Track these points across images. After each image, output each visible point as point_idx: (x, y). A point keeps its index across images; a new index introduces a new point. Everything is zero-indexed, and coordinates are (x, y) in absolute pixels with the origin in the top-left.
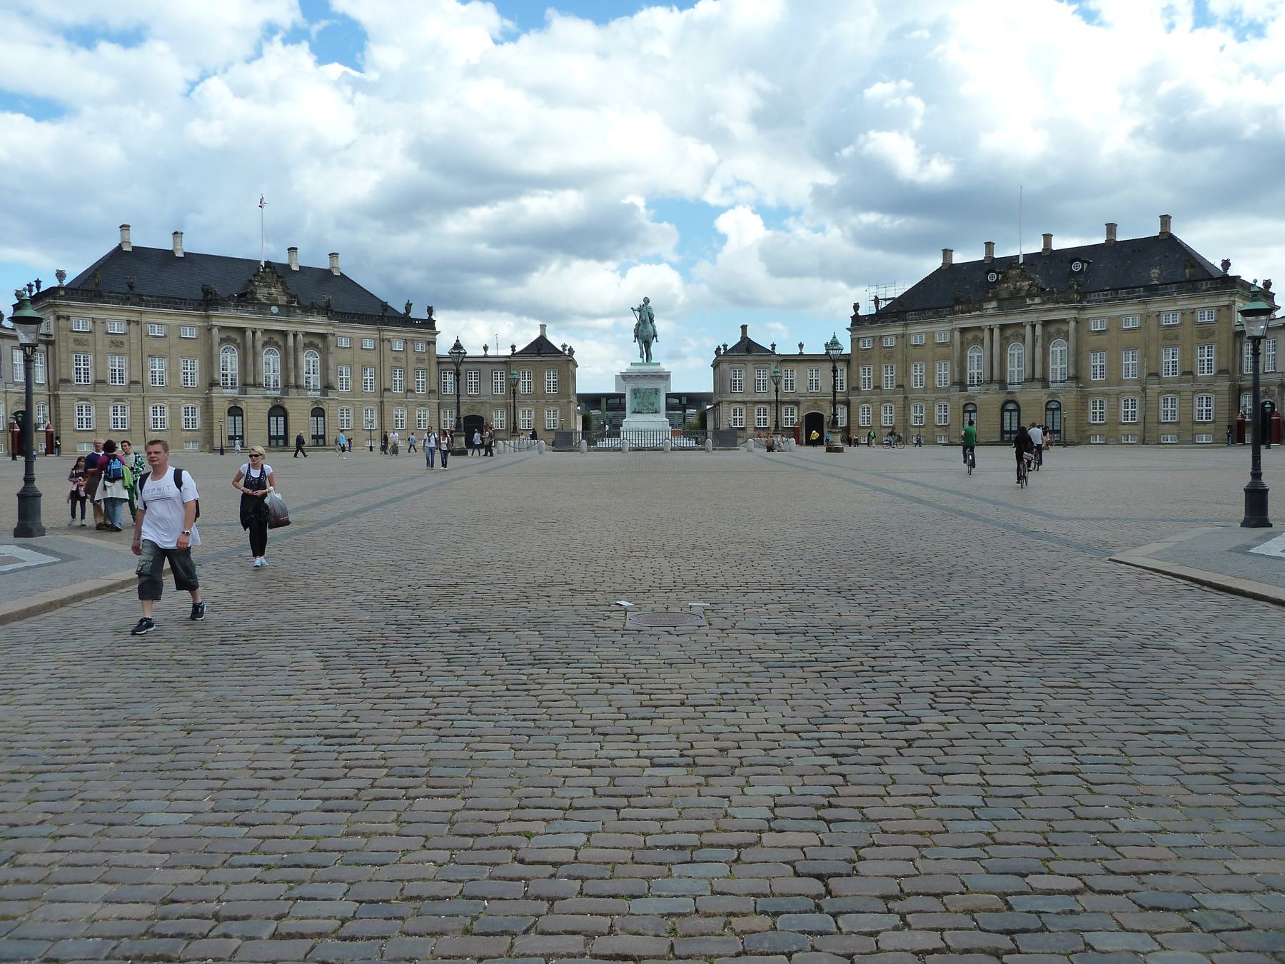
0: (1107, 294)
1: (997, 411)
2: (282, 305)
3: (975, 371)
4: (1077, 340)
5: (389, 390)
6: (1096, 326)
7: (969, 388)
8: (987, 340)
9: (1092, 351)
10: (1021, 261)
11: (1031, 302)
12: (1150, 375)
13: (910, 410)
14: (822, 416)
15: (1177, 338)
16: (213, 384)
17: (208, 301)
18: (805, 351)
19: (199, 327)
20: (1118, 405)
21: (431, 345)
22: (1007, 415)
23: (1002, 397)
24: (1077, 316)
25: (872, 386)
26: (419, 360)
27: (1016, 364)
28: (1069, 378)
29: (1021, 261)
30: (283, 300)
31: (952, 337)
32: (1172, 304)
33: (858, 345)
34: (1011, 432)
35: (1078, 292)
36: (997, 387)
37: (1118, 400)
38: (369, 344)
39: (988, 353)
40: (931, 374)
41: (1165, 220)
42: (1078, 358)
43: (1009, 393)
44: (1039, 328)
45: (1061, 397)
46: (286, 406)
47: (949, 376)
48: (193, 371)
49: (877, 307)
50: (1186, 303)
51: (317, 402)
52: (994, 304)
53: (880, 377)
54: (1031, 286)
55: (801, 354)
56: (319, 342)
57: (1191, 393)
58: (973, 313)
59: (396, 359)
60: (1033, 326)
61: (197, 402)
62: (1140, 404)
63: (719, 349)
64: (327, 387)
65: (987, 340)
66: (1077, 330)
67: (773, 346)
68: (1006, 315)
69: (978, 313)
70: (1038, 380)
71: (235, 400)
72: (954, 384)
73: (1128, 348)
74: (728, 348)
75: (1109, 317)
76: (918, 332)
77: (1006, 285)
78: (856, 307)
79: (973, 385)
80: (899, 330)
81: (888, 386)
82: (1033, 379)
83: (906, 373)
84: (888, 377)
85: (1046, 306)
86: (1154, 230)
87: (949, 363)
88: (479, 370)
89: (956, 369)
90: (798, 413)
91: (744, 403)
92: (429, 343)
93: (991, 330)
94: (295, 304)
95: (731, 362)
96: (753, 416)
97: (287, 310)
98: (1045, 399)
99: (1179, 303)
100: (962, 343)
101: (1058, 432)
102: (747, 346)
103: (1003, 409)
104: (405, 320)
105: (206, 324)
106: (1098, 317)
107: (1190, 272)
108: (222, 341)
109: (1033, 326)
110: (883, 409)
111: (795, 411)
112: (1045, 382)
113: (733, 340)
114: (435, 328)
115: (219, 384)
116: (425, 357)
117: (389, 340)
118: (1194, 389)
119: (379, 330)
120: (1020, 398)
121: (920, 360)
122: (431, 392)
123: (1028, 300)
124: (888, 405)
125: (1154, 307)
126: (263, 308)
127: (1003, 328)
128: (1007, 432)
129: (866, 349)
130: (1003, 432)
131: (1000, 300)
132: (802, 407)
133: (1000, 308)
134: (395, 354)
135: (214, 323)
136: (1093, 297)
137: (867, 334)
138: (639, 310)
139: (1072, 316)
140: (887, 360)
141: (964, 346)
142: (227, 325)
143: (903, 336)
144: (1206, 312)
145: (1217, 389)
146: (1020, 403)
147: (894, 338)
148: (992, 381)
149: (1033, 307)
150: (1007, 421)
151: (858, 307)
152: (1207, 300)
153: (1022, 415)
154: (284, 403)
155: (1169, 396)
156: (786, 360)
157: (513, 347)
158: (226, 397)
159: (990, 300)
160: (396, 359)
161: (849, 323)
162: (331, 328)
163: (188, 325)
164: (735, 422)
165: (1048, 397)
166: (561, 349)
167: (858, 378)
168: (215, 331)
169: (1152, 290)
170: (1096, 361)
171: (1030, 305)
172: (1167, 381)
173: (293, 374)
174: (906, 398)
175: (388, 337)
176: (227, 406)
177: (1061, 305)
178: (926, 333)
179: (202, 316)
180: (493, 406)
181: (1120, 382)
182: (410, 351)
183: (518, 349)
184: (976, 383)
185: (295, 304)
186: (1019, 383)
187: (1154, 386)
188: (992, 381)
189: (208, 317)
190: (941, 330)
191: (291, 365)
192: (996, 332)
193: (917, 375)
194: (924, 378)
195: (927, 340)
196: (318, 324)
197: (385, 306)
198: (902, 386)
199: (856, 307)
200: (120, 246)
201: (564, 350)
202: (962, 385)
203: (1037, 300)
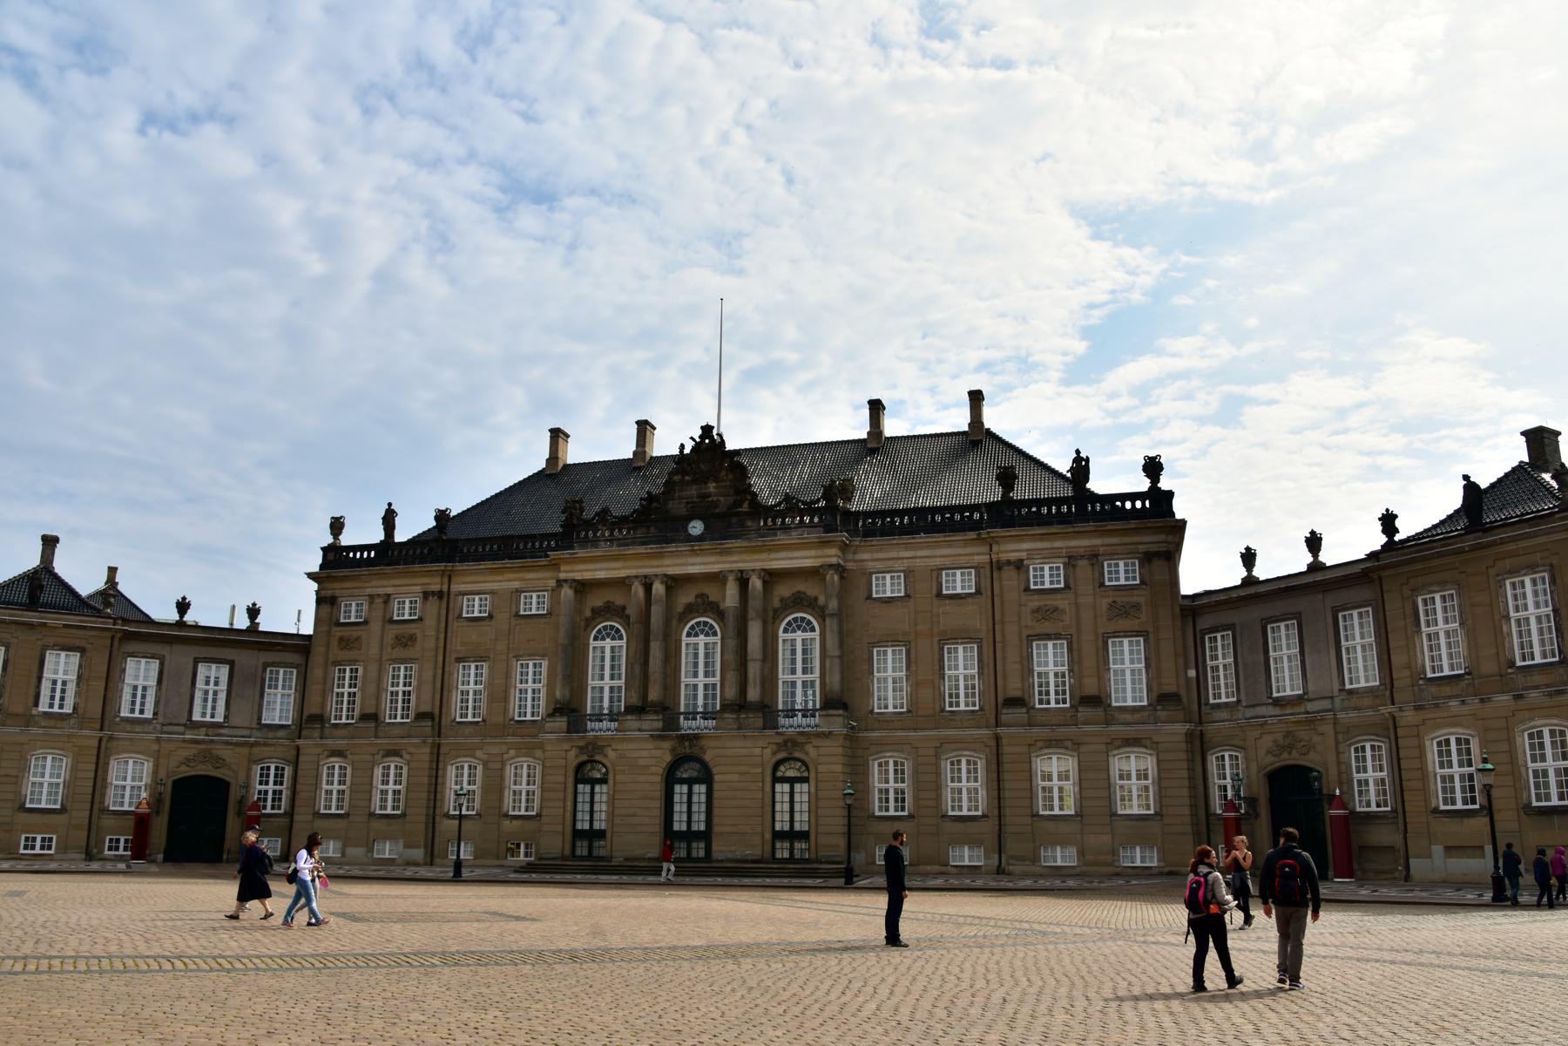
14: (228, 784)
22: (680, 790)
34: (690, 836)
43: (683, 738)
45: (812, 752)
47: (543, 695)
53: (379, 689)
60: (743, 581)
78: (337, 526)
81: (395, 715)
83: (443, 687)
101: (804, 836)
103: (670, 780)
128: (681, 835)
130: (669, 833)
150: (679, 808)
153: (716, 794)
161: (315, 562)
165: (774, 753)
186: (706, 715)
194: (484, 697)
199: (337, 526)
202: (569, 711)
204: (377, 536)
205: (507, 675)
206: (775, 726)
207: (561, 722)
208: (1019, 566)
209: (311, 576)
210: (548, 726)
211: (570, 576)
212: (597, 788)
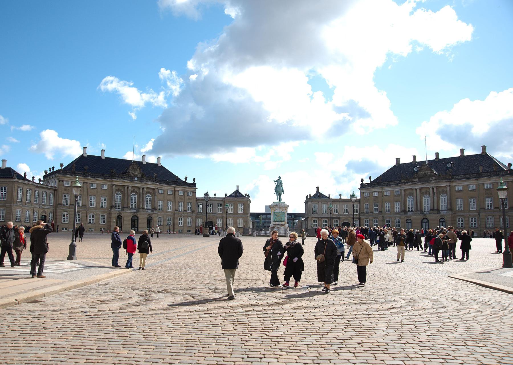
1: (420, 222)
2: (139, 177)
3: (410, 206)
4: (450, 194)
5: (177, 210)
6: (458, 189)
7: (408, 213)
8: (415, 194)
9: (457, 199)
10: (427, 163)
11: (431, 179)
12: (481, 208)
13: (384, 222)
15: (491, 194)
16: (112, 207)
17: (111, 176)
18: (342, 197)
19: (108, 185)
20: (469, 221)
21: (194, 193)
23: (421, 217)
24: (450, 185)
25: (369, 212)
26: (189, 199)
27: (426, 203)
28: (448, 209)
29: (427, 163)
30: (139, 175)
31: (401, 192)
33: (363, 195)
35: (450, 175)
36: (419, 212)
37: (469, 218)
38: (170, 192)
39: (415, 199)
40: (393, 207)
41: (484, 148)
42: (451, 202)
43: (424, 215)
44: (435, 189)
45: (445, 217)
46: (138, 216)
47: (400, 208)
48: (105, 202)
49: (370, 180)
50: (494, 180)
51: (150, 214)
52: (417, 180)
53: (372, 208)
54: (431, 173)
55: (340, 199)
56: (152, 192)
57: (499, 216)
58: (409, 183)
59: (180, 198)
60: (433, 189)
61: (106, 213)
62: (478, 220)
63: (307, 196)
64: (154, 209)
65: (415, 194)
66: (450, 190)
67: (329, 195)
68: (422, 184)
69: (410, 183)
70: (436, 210)
71: (119, 213)
72: (402, 211)
73: (471, 198)
74: (311, 196)
75: (463, 185)
76: (387, 191)
77: (421, 172)
78: (362, 180)
79: (410, 212)
80: (379, 189)
82: (434, 210)
84: (375, 208)
85: (438, 181)
86: (479, 152)
87: (400, 203)
89: (403, 205)
90: (339, 222)
91: (318, 218)
92: (193, 192)
93: (416, 190)
94: (144, 177)
95: (312, 202)
96: (321, 223)
97: (141, 179)
98: (439, 218)
99: (491, 180)
100: (405, 195)
102: (319, 195)
103: (422, 222)
104: (184, 183)
105: (111, 184)
106: (458, 185)
107: (495, 168)
108: (116, 190)
109: (433, 189)
110: (374, 221)
111: (338, 221)
112: (438, 211)
113: (313, 192)
114: (196, 187)
115: (114, 207)
116: (191, 198)
117: (178, 191)
118: (500, 215)
119: (174, 187)
120: (429, 217)
121: (388, 202)
122: (193, 211)
123: (430, 178)
124: (376, 219)
125: (482, 181)
126: (132, 178)
127: (421, 189)
129: (366, 197)
131: (419, 178)
134: (180, 197)
135: (114, 184)
136: (456, 177)
137: (367, 191)
138: (277, 181)
139: (448, 185)
141: (406, 196)
142: (118, 184)
143: (381, 192)
145: (510, 214)
147: (378, 193)
148: (417, 210)
151: (363, 180)
154: (137, 215)
155: (490, 217)
156: (335, 201)
157: (226, 194)
158: (116, 212)
159: (415, 178)
160: (180, 198)
161: (359, 187)
162: (156, 186)
163: (104, 184)
164: (314, 226)
166: (245, 195)
167: (364, 208)
168: (114, 186)
169: (480, 175)
170: (459, 202)
172: (490, 211)
173: (141, 203)
174: (383, 216)
175: (178, 190)
176: (116, 215)
177: (444, 180)
178: (390, 191)
179: (110, 181)
180: (217, 218)
181: (469, 211)
182: (186, 195)
183: (228, 195)
184: (411, 211)
185: (144, 177)
186: (428, 211)
187: (483, 213)
188: (417, 210)
189: (112, 181)
190: (396, 190)
191: (141, 200)
192: (418, 191)
193: (387, 207)
194: (390, 208)
195: (391, 193)
196: (152, 185)
197: (177, 178)
198: (381, 212)
199: (362, 180)
200: (82, 155)
201: (246, 196)
203: (434, 178)
204: (369, 182)
205: (394, 204)
206: (440, 213)
207: (403, 213)
208: (483, 184)
209: (359, 189)
210: (401, 213)
211: (403, 188)
212: (410, 224)
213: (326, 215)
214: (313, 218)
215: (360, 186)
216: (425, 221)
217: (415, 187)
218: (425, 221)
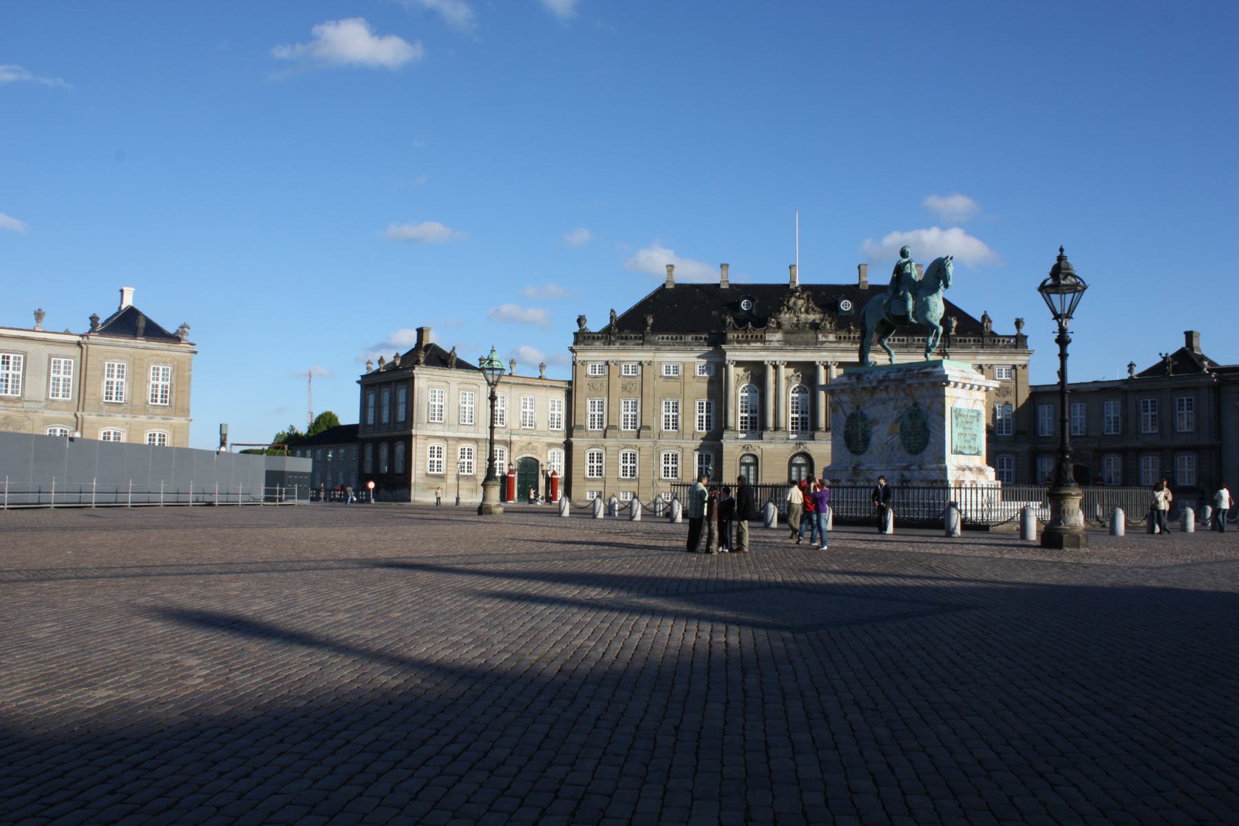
0: (903, 340)
11: (824, 339)
22: (794, 469)
32: (971, 357)
47: (712, 419)
52: (779, 336)
68: (795, 351)
69: (758, 344)
88: (25, 354)
91: (446, 439)
93: (776, 367)
129: (596, 377)
131: (786, 332)
132: (515, 448)
133: (786, 342)
137: (595, 356)
140: (626, 393)
144: (1004, 370)
146: (813, 456)
149: (826, 345)
152: (1005, 357)
171: (823, 342)
199: (580, 320)
203: (831, 337)
213: (472, 429)
214: (430, 440)
215: (572, 339)
216: (799, 462)
217: (774, 359)
218: (799, 460)
